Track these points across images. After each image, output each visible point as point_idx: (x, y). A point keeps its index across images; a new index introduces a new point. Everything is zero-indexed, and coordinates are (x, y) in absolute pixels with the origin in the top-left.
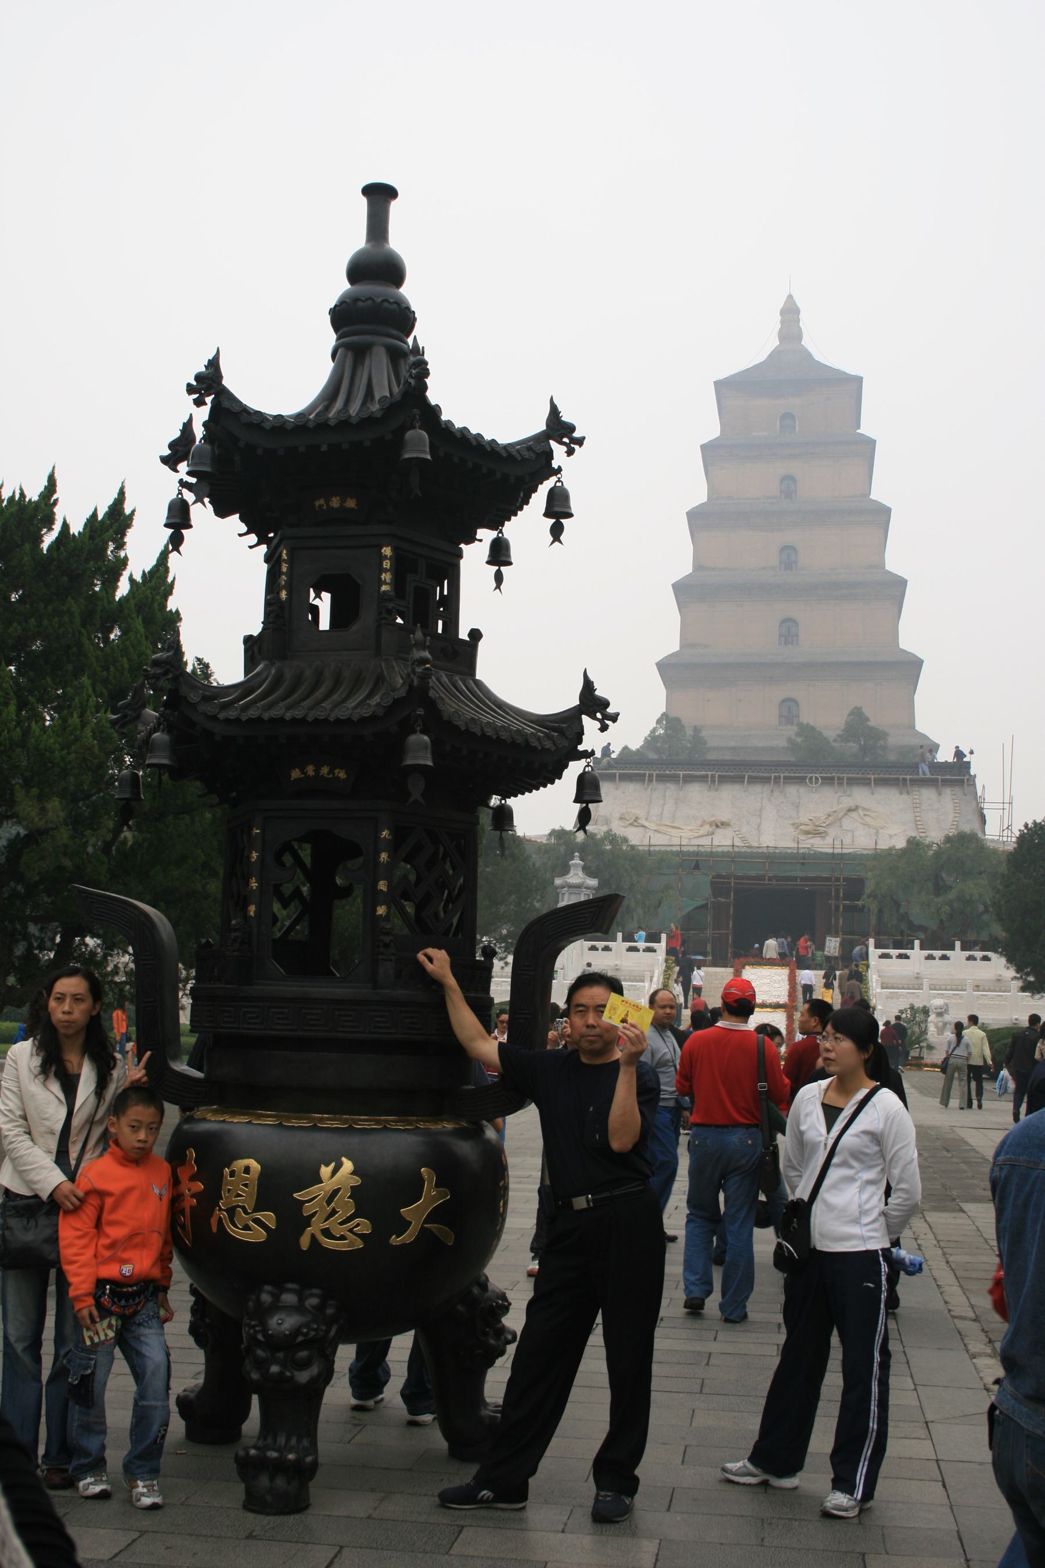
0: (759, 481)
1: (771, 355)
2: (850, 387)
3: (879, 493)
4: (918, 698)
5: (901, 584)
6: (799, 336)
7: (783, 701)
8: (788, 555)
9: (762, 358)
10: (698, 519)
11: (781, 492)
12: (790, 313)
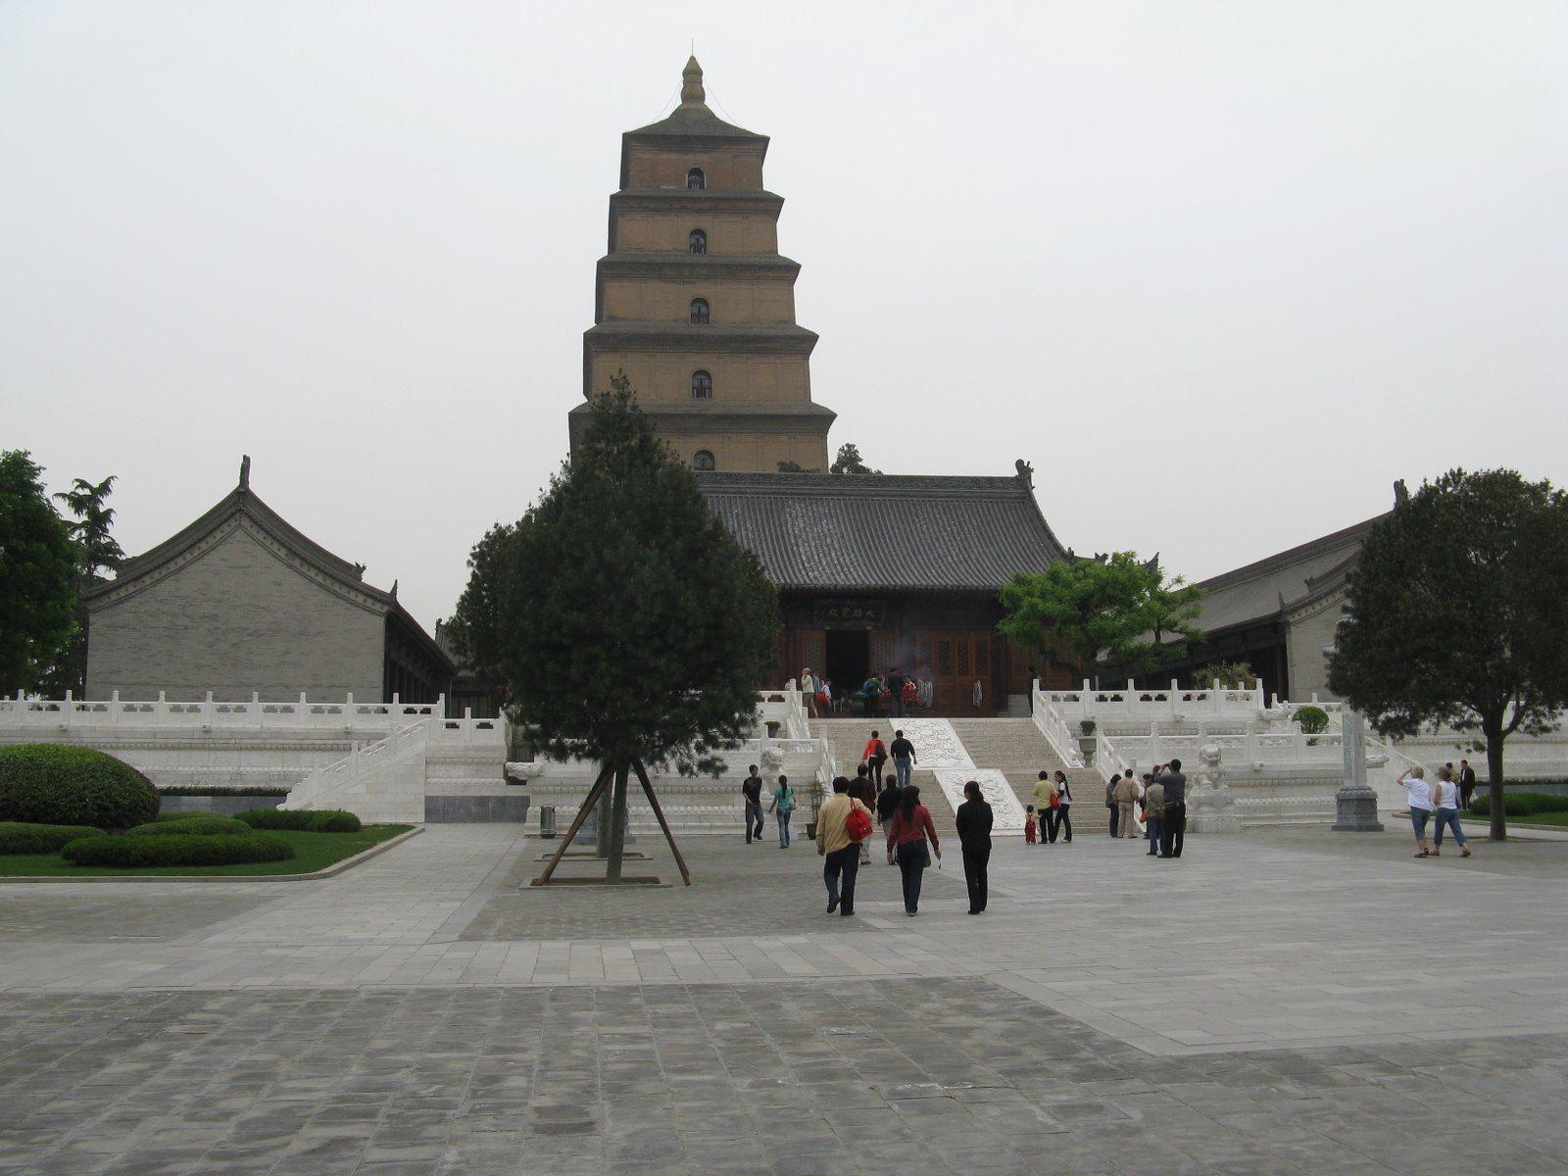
0: (666, 234)
1: (675, 113)
3: (786, 249)
6: (702, 97)
7: (700, 453)
8: (700, 308)
9: (666, 115)
11: (691, 245)
12: (693, 74)
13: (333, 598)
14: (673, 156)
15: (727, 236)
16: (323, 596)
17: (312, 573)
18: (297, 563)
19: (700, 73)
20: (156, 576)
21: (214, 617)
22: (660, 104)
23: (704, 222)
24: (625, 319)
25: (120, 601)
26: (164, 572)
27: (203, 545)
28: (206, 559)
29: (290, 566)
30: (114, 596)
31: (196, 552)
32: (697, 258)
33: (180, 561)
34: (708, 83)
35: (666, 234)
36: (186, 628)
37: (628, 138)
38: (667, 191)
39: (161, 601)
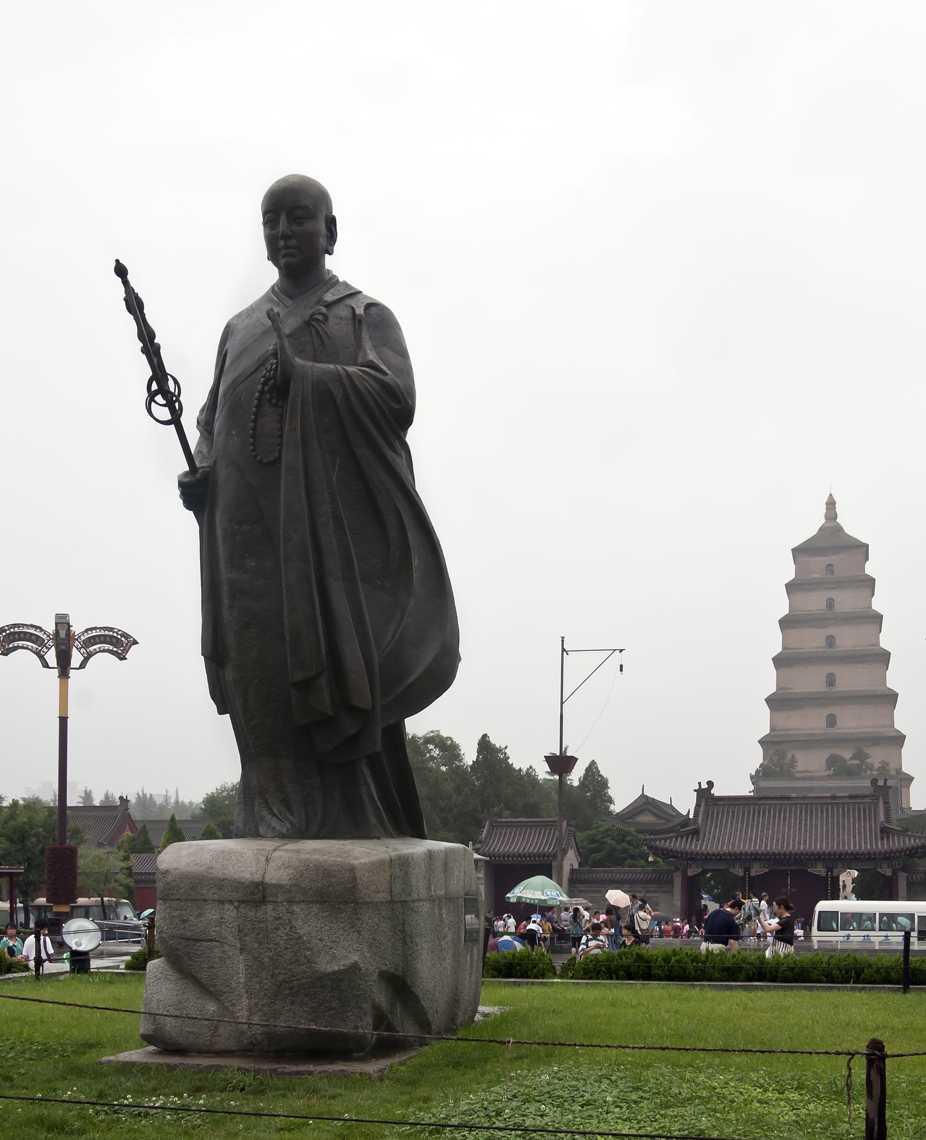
2: (862, 550)
4: (896, 712)
5: (888, 654)
6: (836, 517)
8: (831, 641)
10: (785, 623)
12: (831, 504)
14: (818, 558)
19: (834, 503)
22: (810, 525)
23: (834, 594)
24: (792, 649)
34: (839, 509)
35: (815, 602)
37: (795, 551)
38: (814, 578)
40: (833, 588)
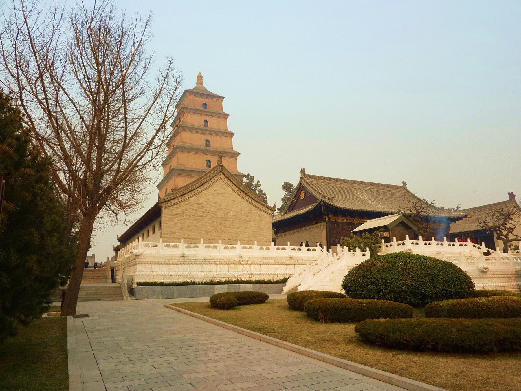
13: (254, 208)
15: (214, 123)
16: (251, 206)
17: (247, 198)
18: (242, 193)
20: (190, 195)
21: (212, 213)
25: (175, 204)
26: (193, 193)
27: (207, 184)
28: (209, 190)
29: (239, 195)
30: (173, 202)
31: (205, 187)
32: (206, 128)
33: (199, 190)
36: (202, 216)
39: (191, 205)
40: (207, 115)
